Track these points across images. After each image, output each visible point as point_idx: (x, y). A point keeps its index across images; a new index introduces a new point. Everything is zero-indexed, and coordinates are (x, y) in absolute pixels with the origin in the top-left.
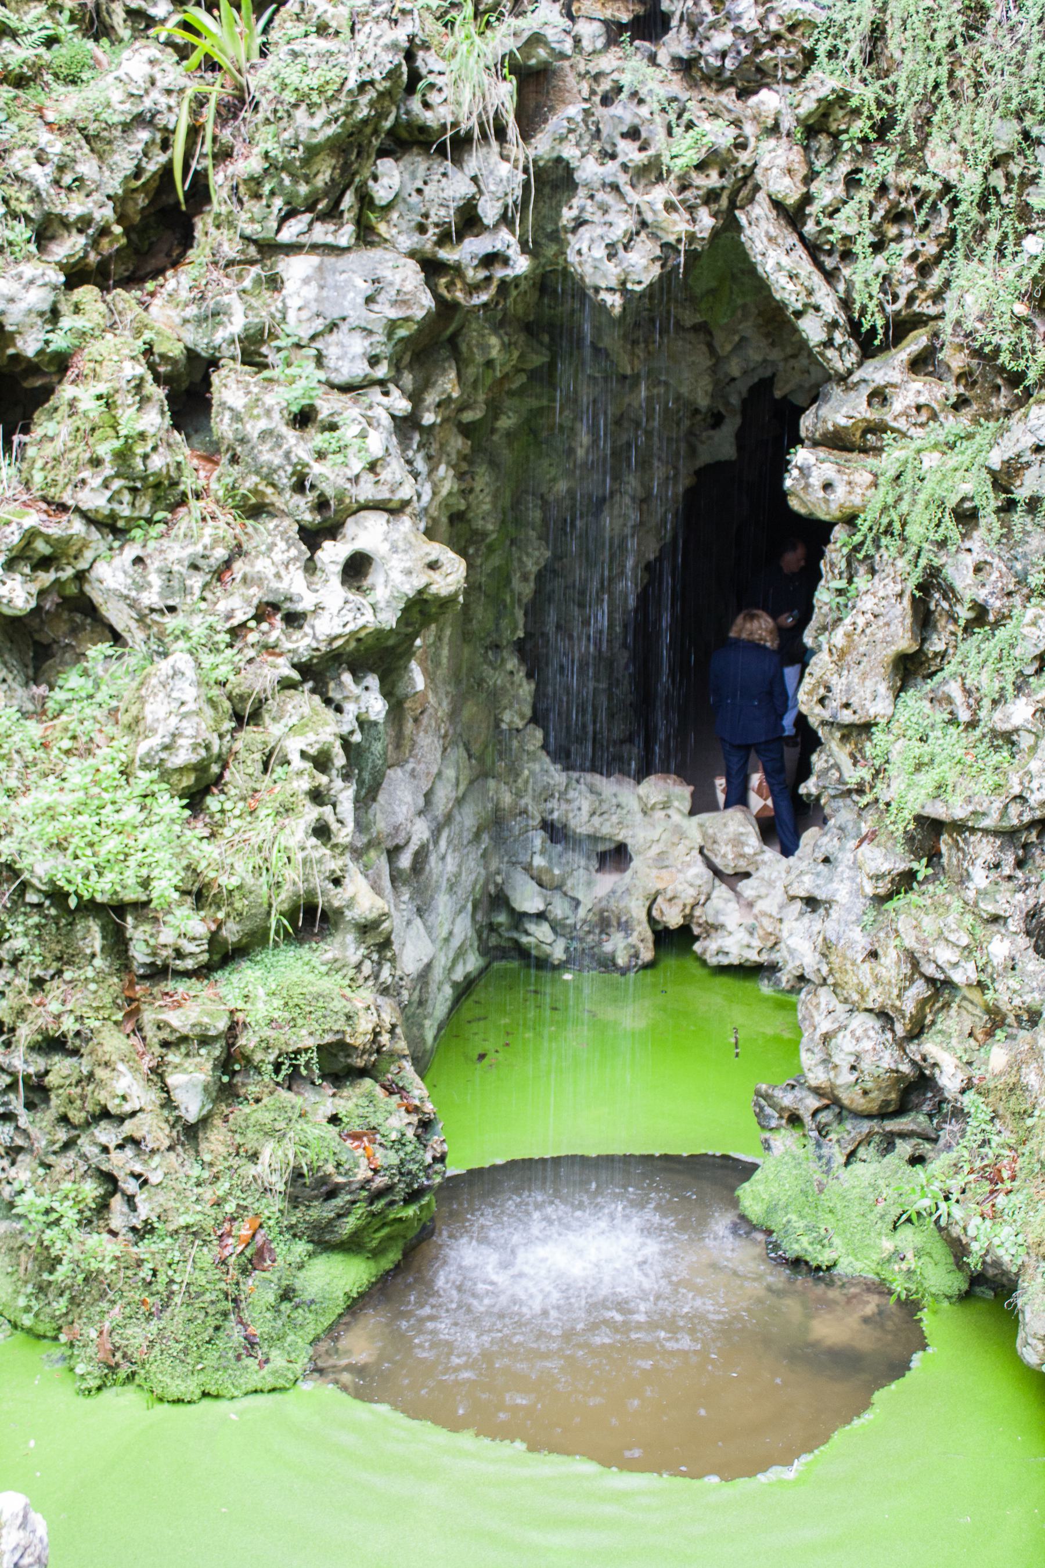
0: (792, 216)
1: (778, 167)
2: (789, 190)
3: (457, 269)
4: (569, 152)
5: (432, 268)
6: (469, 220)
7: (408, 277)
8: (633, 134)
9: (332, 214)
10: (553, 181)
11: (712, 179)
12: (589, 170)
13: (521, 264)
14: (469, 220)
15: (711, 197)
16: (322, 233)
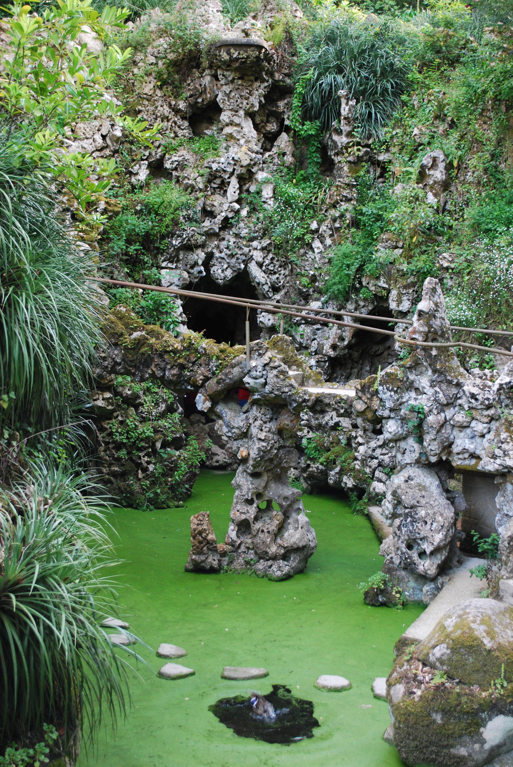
0: (260, 265)
1: (258, 256)
2: (260, 260)
3: (193, 274)
4: (215, 251)
5: (189, 273)
6: (196, 264)
7: (185, 275)
8: (227, 248)
9: (172, 262)
10: (210, 256)
11: (244, 258)
12: (217, 254)
13: (204, 274)
14: (196, 264)
15: (244, 261)
16: (170, 265)
